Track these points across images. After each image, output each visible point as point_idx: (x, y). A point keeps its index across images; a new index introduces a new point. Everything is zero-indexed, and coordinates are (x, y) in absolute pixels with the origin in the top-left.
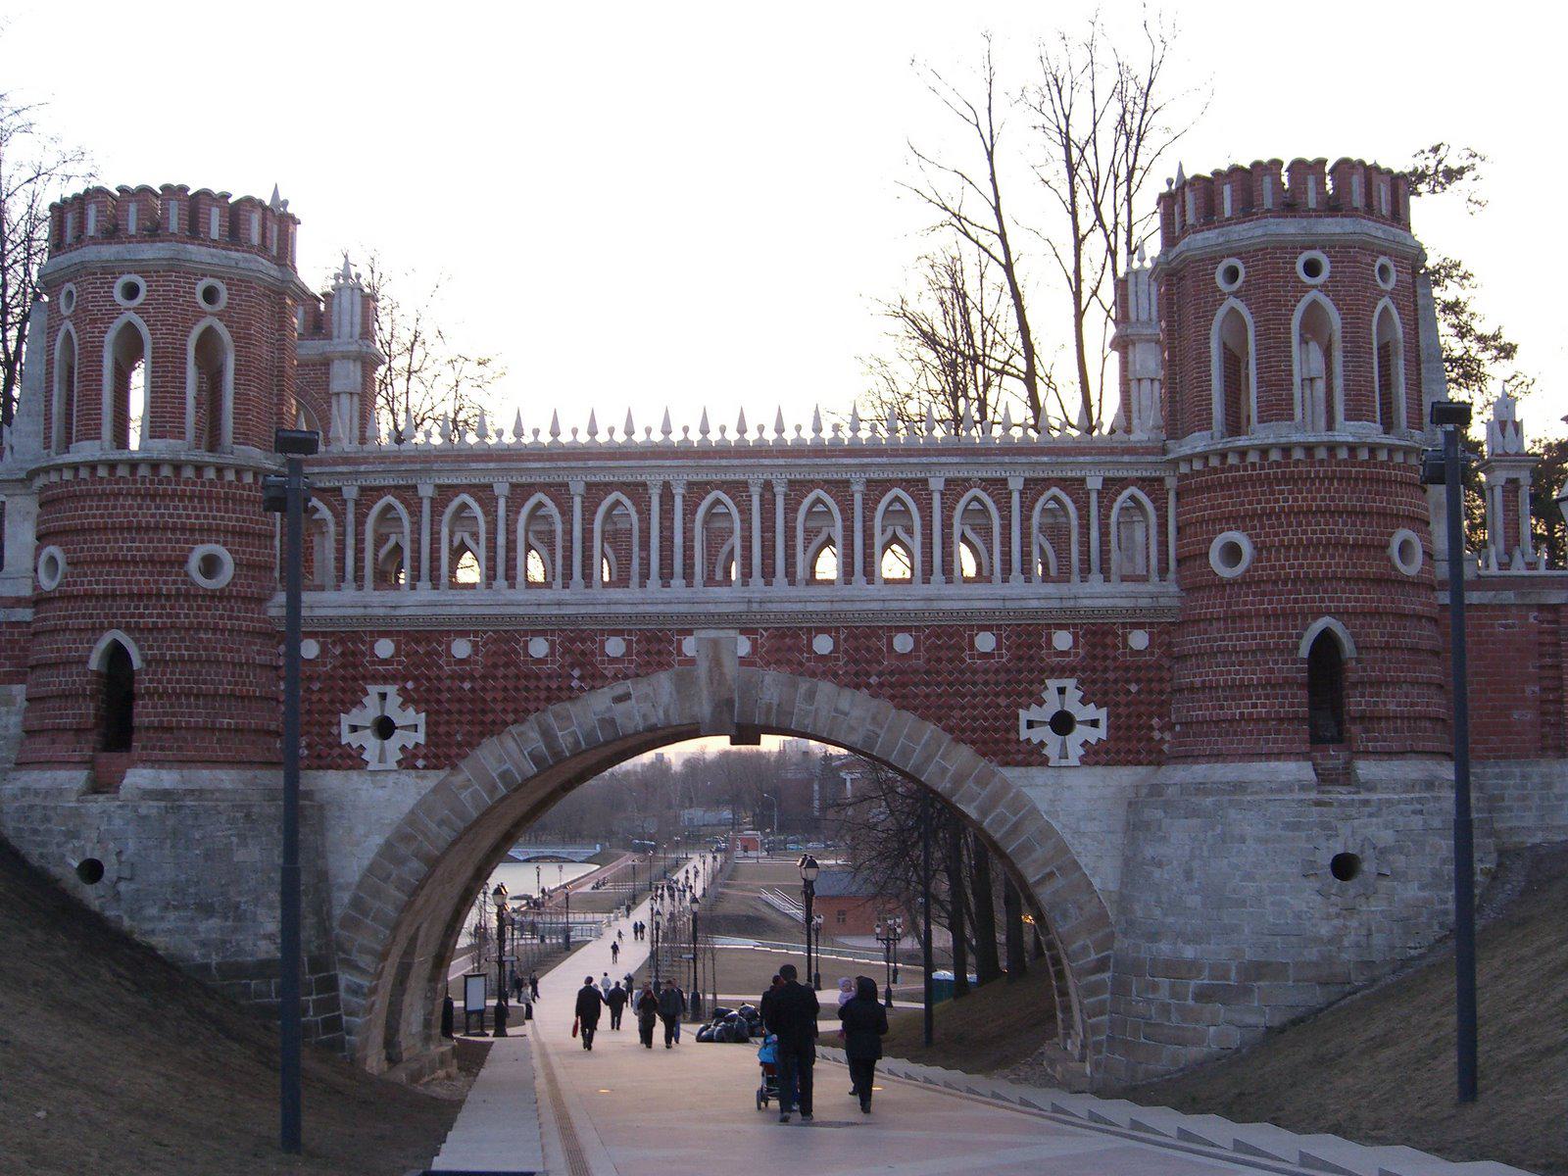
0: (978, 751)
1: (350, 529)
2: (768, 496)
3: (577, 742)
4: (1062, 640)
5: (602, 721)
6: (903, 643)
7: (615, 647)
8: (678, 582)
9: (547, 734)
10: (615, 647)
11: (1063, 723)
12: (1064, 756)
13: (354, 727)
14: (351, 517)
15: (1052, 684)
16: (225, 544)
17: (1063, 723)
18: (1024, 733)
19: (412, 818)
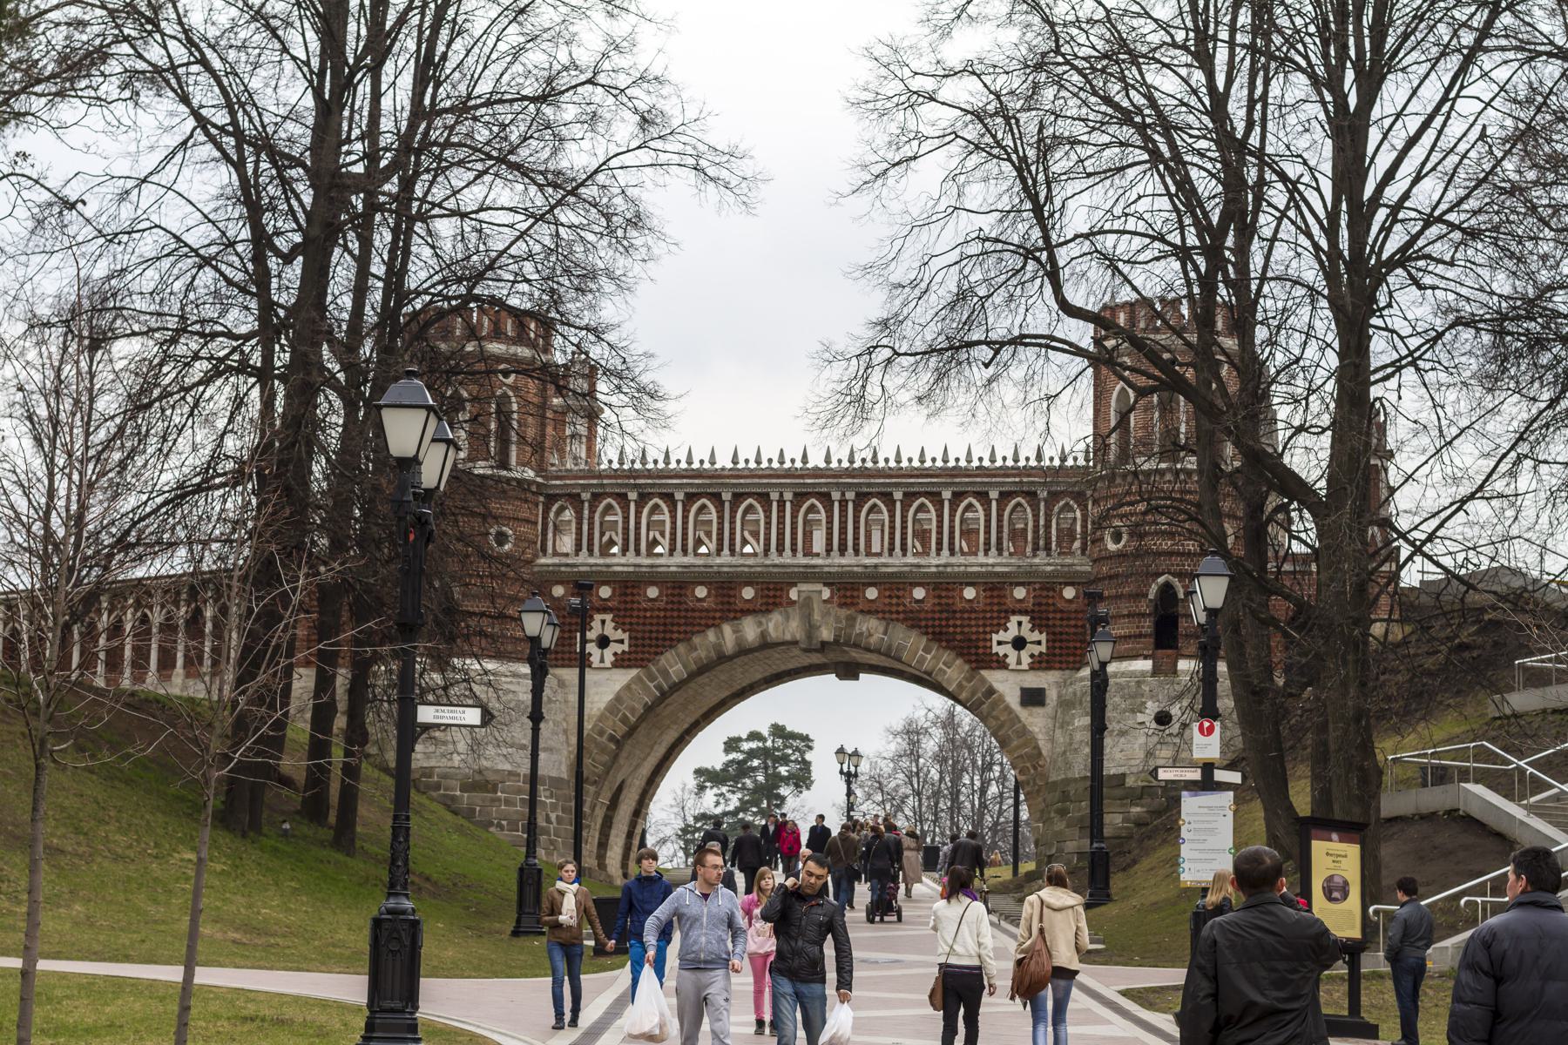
4: (1020, 593)
7: (748, 593)
10: (748, 593)
11: (1019, 643)
12: (1019, 662)
14: (586, 512)
15: (1014, 619)
17: (1019, 643)
18: (995, 649)
19: (618, 698)
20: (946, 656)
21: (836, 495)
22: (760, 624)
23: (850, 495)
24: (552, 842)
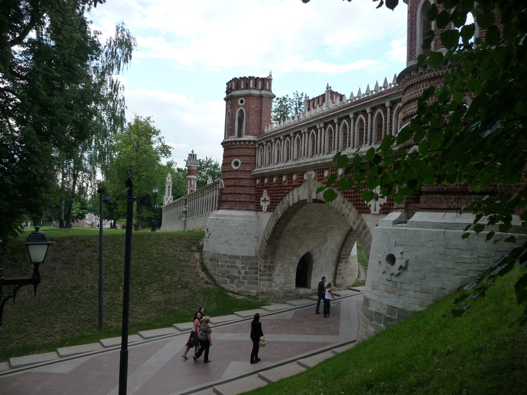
16: (239, 159)
20: (350, 205)
21: (318, 127)
22: (298, 192)
23: (322, 125)
24: (240, 282)
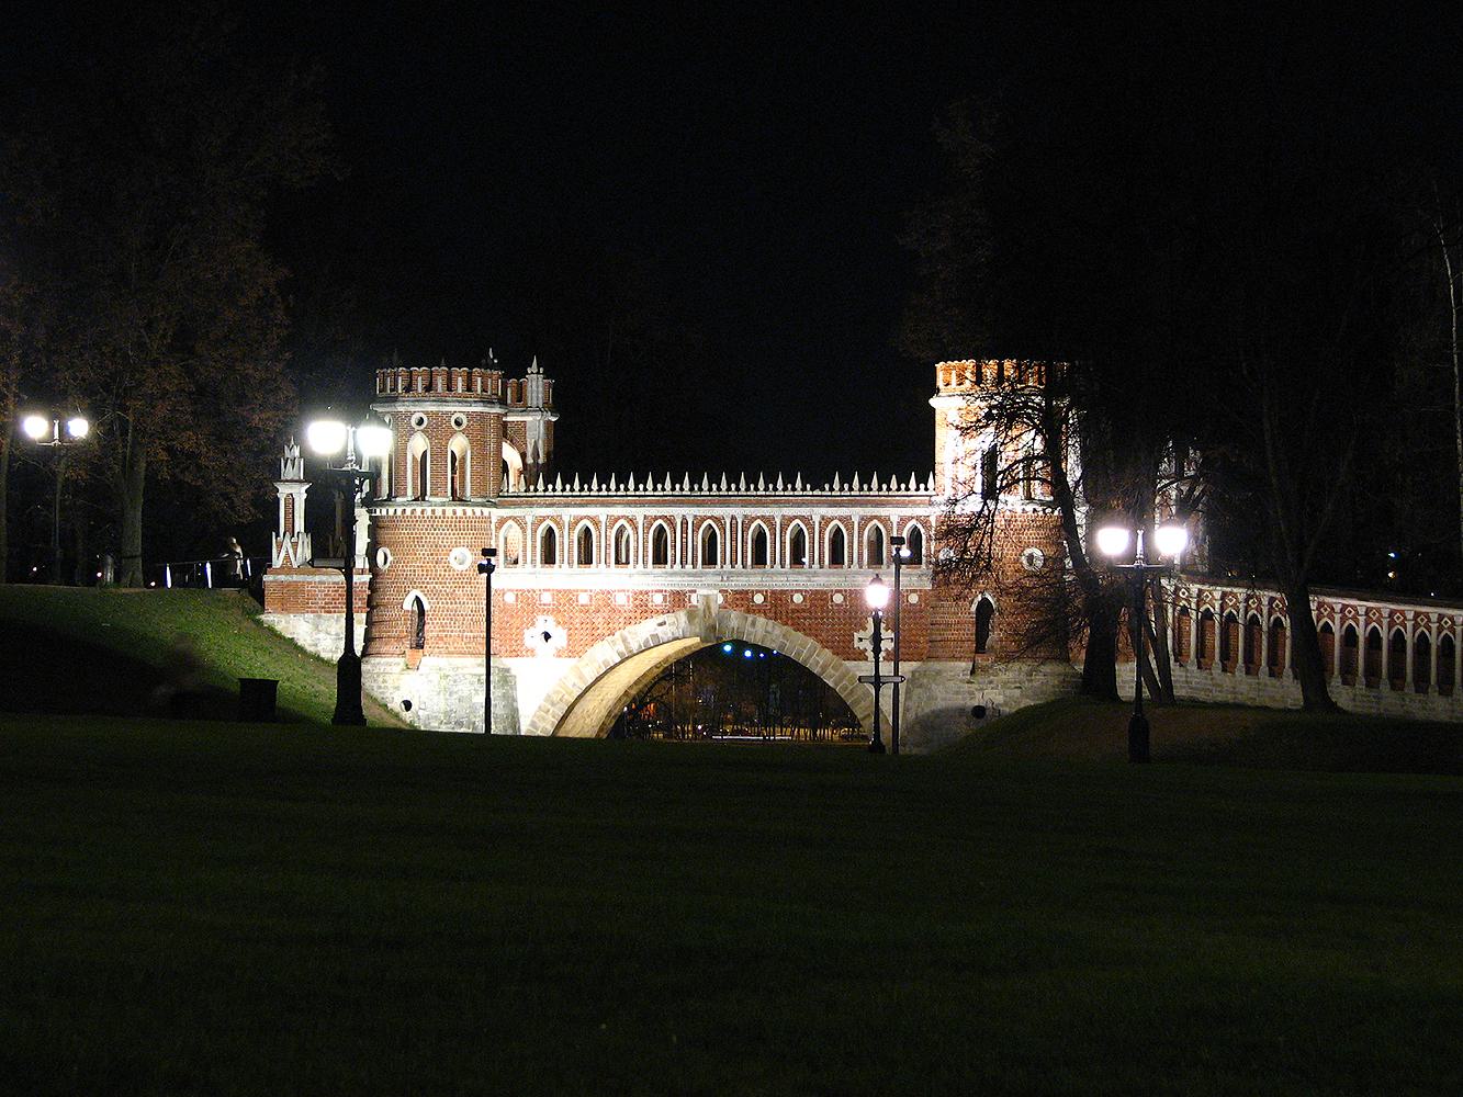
0: (834, 654)
1: (529, 537)
2: (734, 522)
3: (640, 646)
5: (652, 636)
6: (798, 598)
8: (689, 567)
9: (624, 641)
10: (658, 599)
13: (532, 637)
14: (529, 532)
